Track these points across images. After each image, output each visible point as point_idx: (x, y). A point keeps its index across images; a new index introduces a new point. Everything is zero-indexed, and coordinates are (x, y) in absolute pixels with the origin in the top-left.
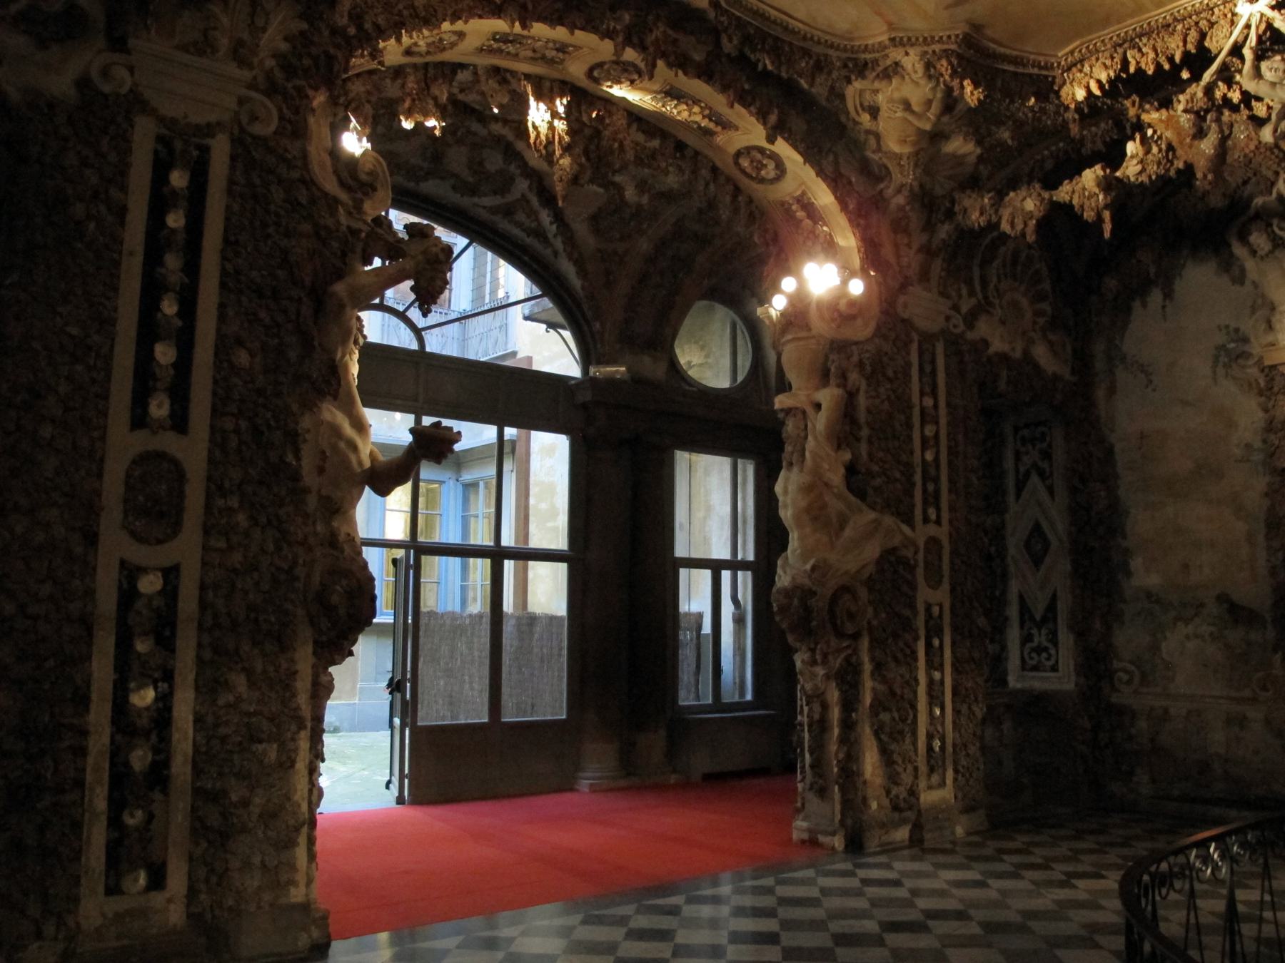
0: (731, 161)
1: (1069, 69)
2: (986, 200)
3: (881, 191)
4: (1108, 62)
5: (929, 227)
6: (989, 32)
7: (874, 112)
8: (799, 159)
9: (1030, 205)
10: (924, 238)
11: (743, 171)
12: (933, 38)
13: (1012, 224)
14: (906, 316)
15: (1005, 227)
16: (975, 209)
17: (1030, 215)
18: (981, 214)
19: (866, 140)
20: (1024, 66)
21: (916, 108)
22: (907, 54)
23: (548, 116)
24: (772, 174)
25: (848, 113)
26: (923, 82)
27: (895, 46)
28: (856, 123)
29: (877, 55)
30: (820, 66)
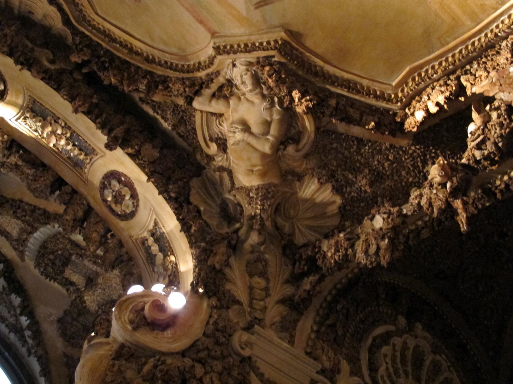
1: (408, 104)
3: (237, 231)
5: (295, 279)
6: (309, 43)
7: (223, 145)
11: (105, 201)
12: (254, 44)
13: (366, 252)
17: (381, 235)
18: (337, 251)
19: (221, 178)
20: (358, 92)
25: (202, 150)
26: (256, 99)
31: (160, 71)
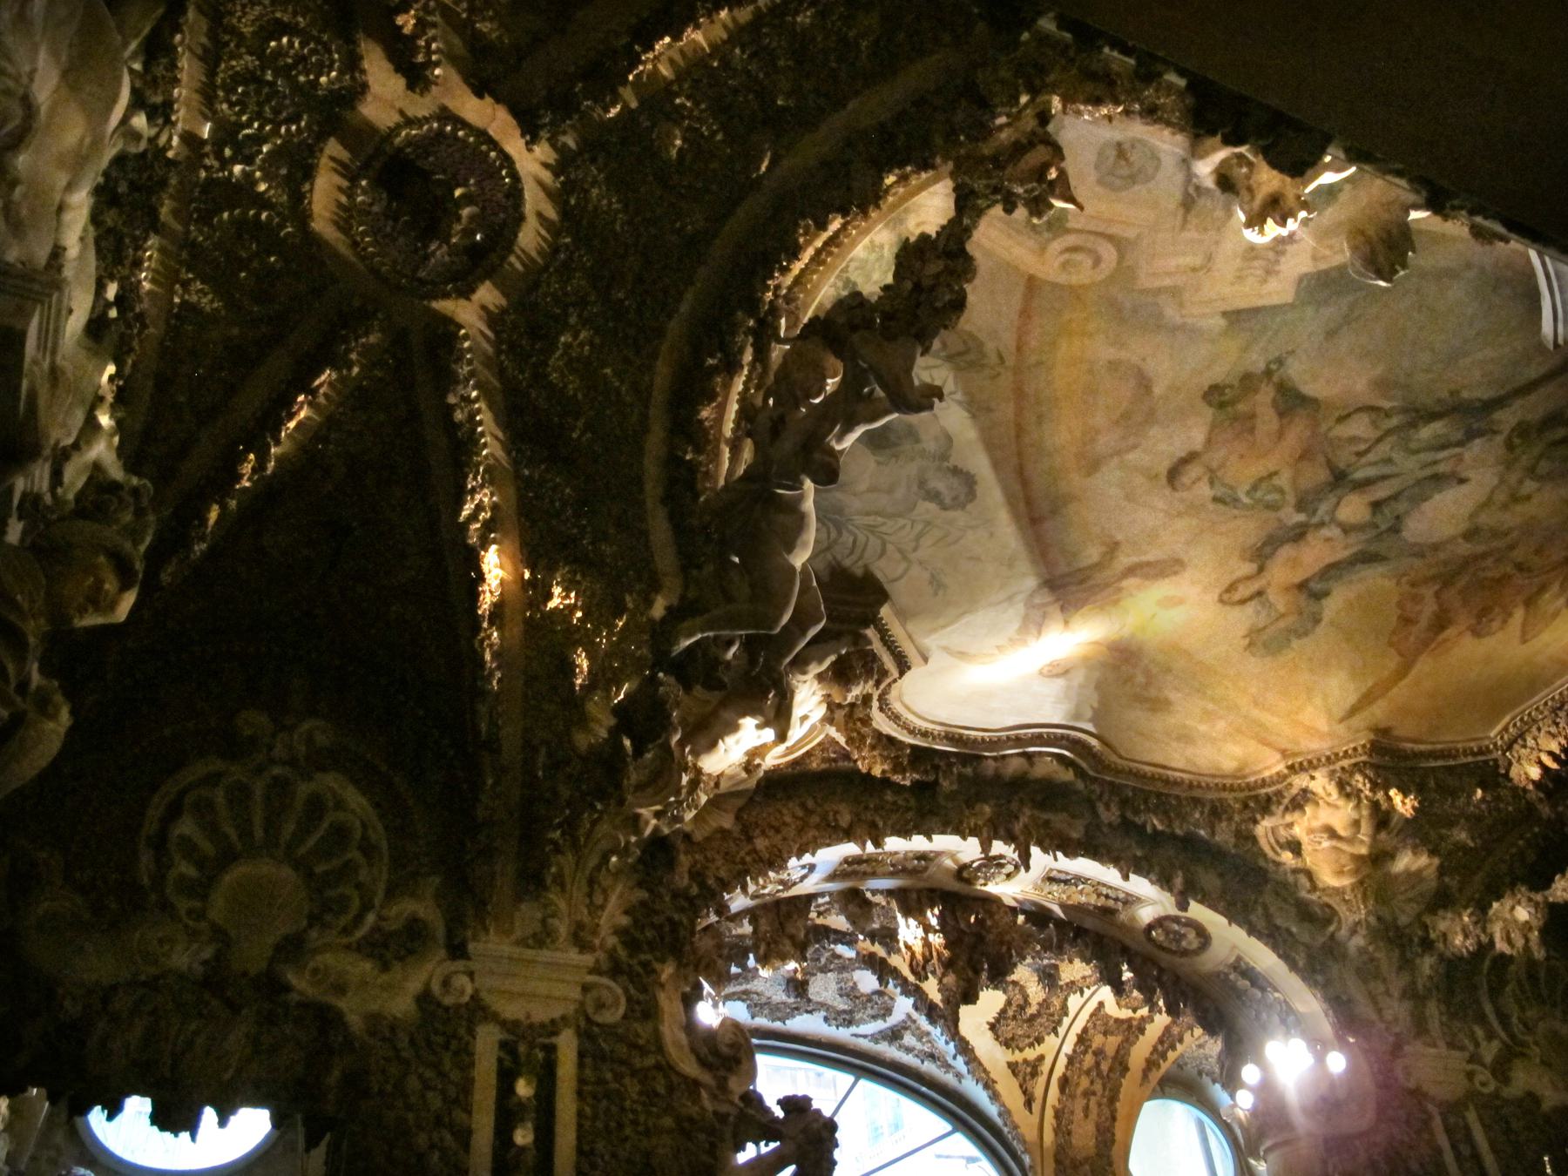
0: (1142, 938)
1: (1510, 747)
2: (1466, 919)
3: (1332, 936)
4: (1553, 729)
5: (1406, 964)
7: (1295, 847)
8: (1223, 920)
9: (1522, 914)
10: (1404, 979)
12: (1337, 755)
13: (1509, 941)
14: (1412, 1085)
15: (1501, 946)
16: (1457, 933)
17: (1527, 927)
18: (1466, 936)
21: (1342, 833)
22: (1313, 778)
23: (920, 932)
24: (1195, 945)
25: (1265, 856)
26: (1341, 803)
27: (1296, 773)
28: (1278, 864)
29: (1279, 787)
30: (1217, 812)
31: (1211, 796)
